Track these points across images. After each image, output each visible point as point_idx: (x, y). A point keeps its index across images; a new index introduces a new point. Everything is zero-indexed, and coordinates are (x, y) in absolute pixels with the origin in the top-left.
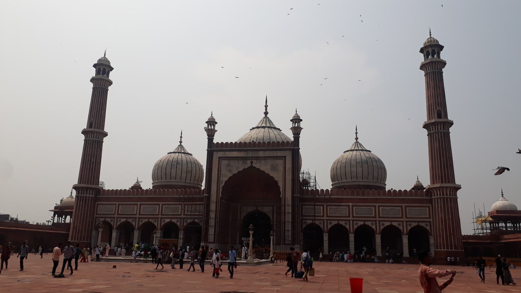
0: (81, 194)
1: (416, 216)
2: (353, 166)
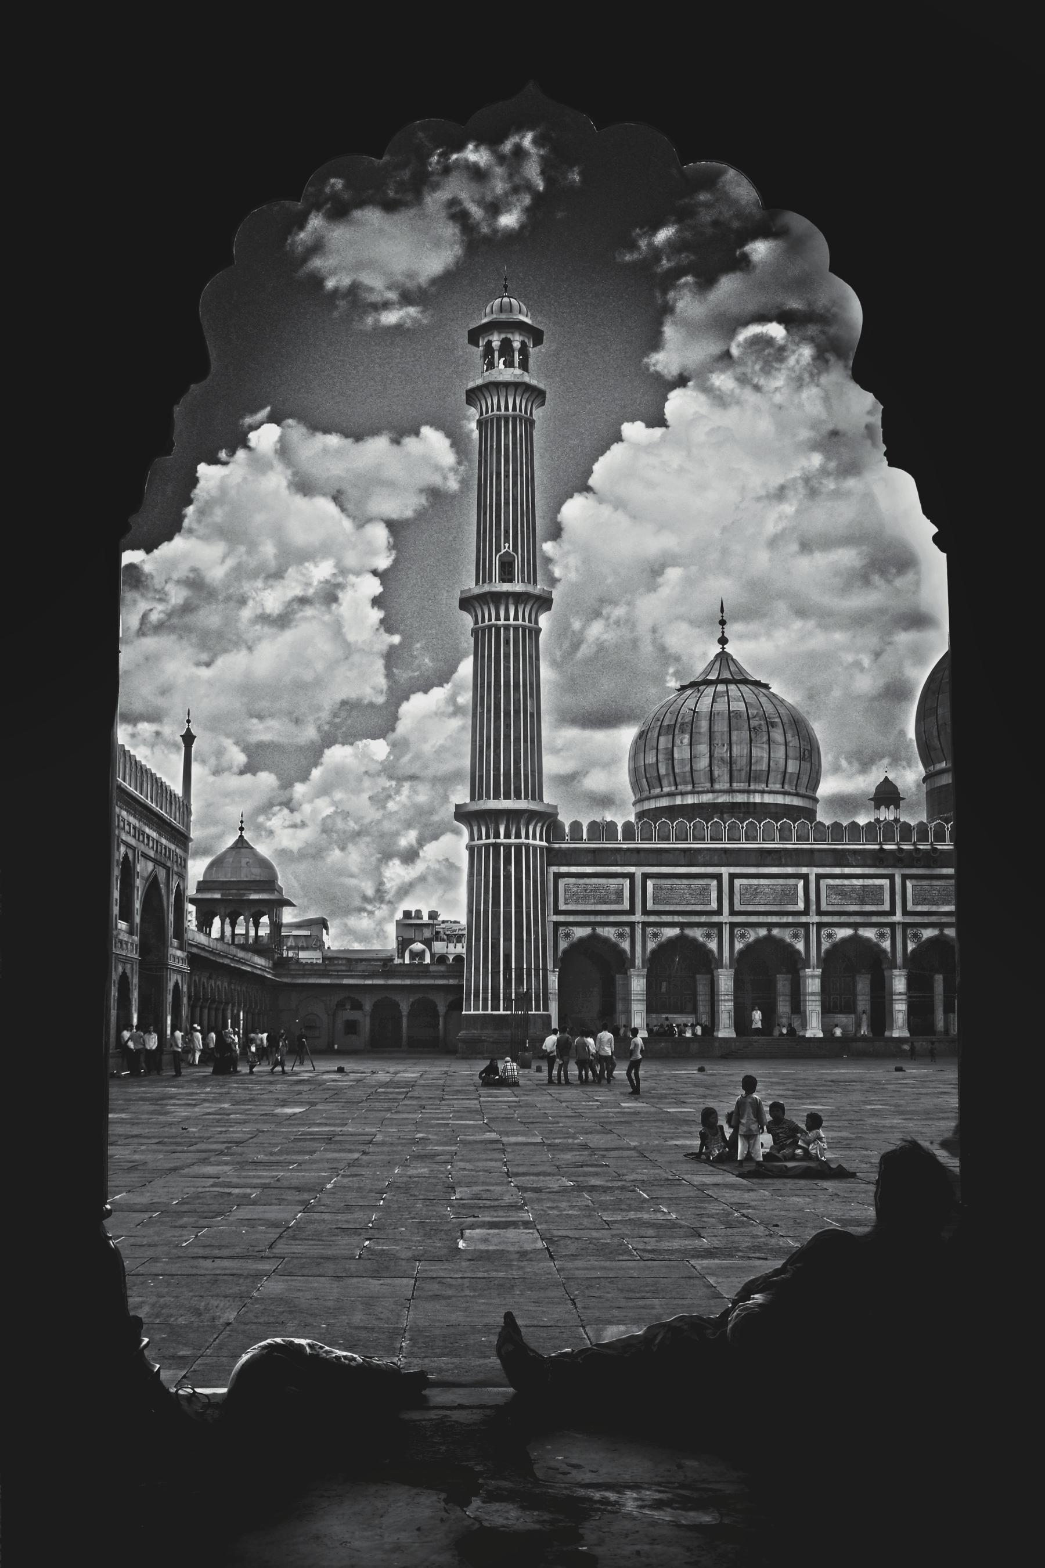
0: (507, 836)
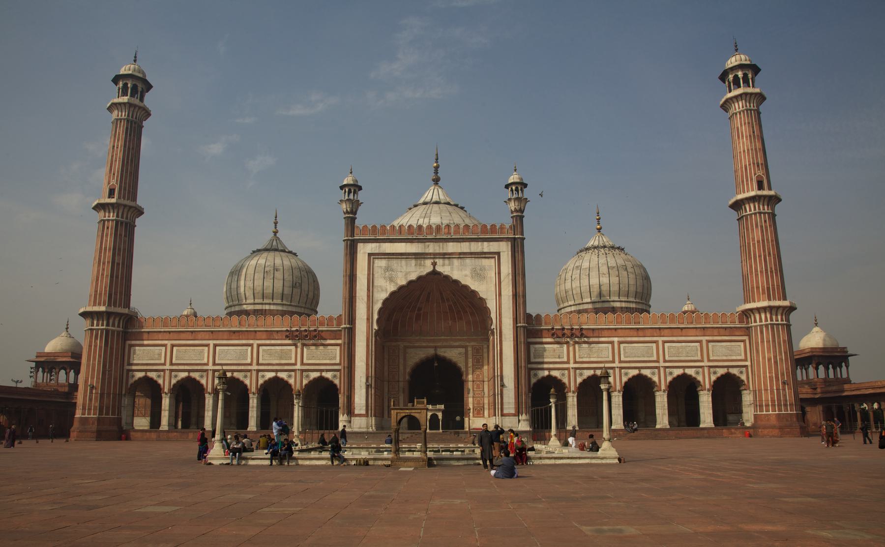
0: (98, 325)
1: (725, 358)
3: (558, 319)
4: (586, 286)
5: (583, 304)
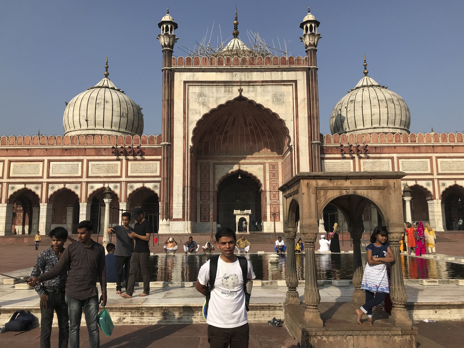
2: (374, 106)
3: (345, 139)
4: (360, 116)
5: (357, 130)
